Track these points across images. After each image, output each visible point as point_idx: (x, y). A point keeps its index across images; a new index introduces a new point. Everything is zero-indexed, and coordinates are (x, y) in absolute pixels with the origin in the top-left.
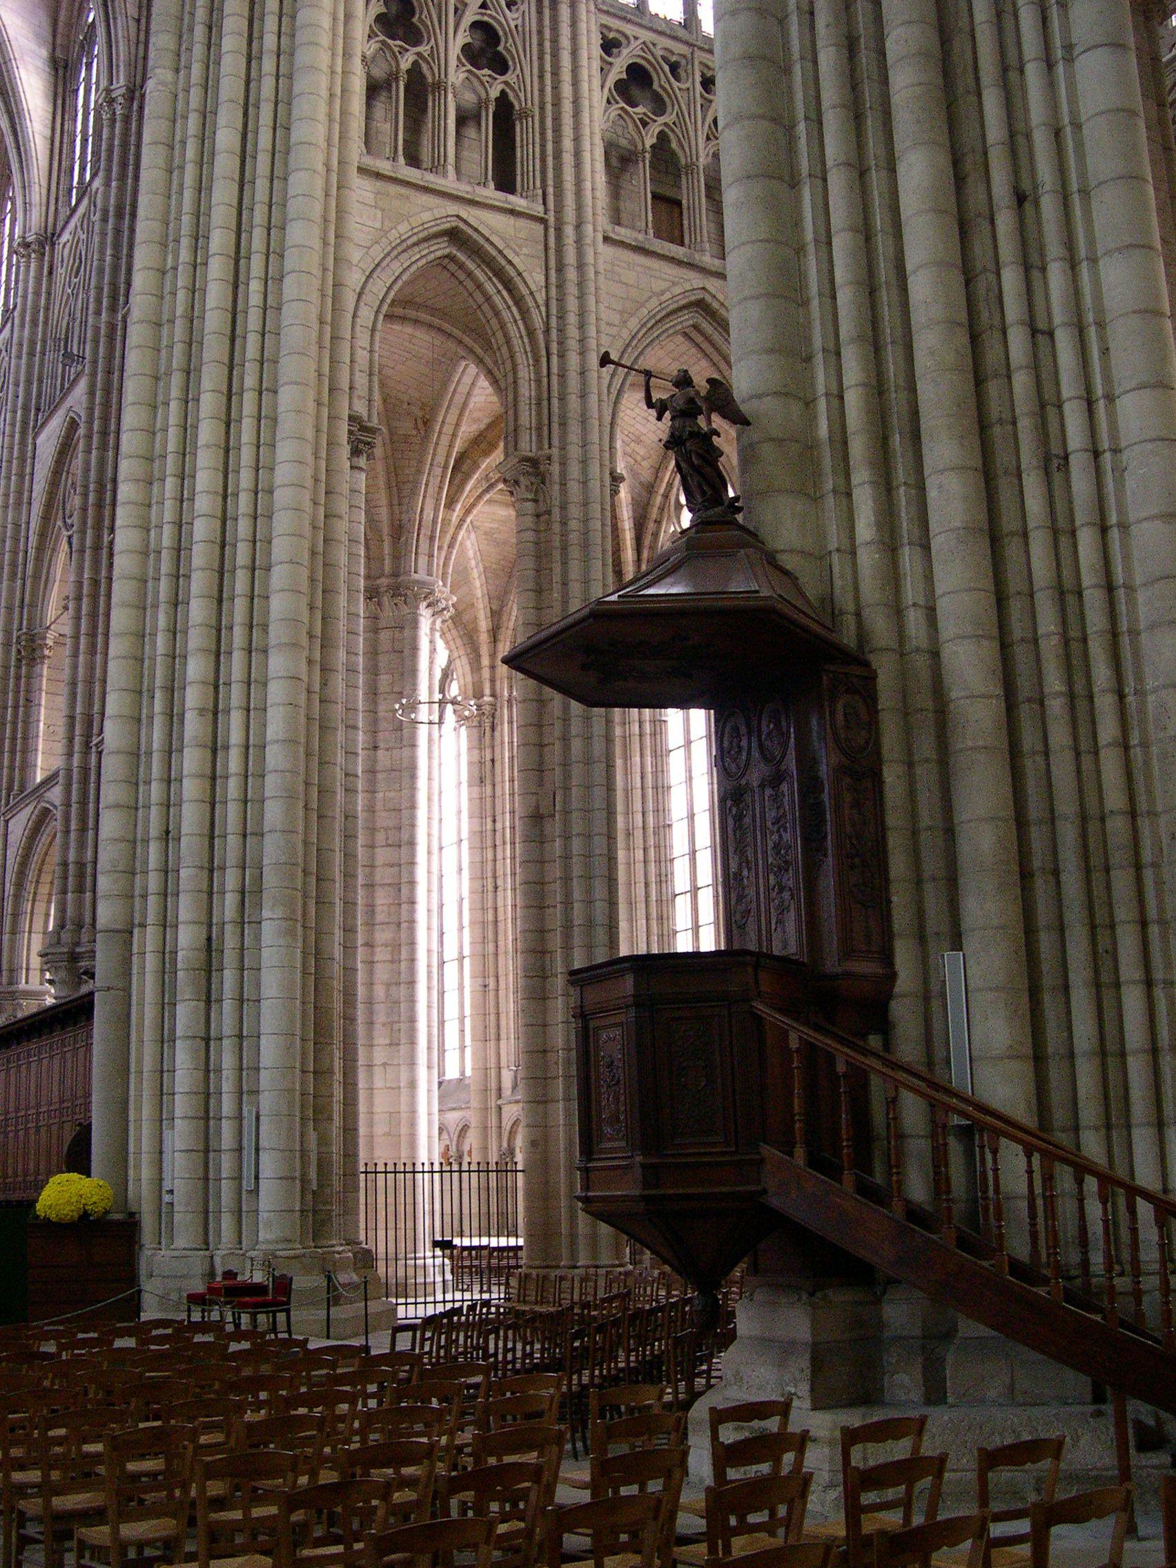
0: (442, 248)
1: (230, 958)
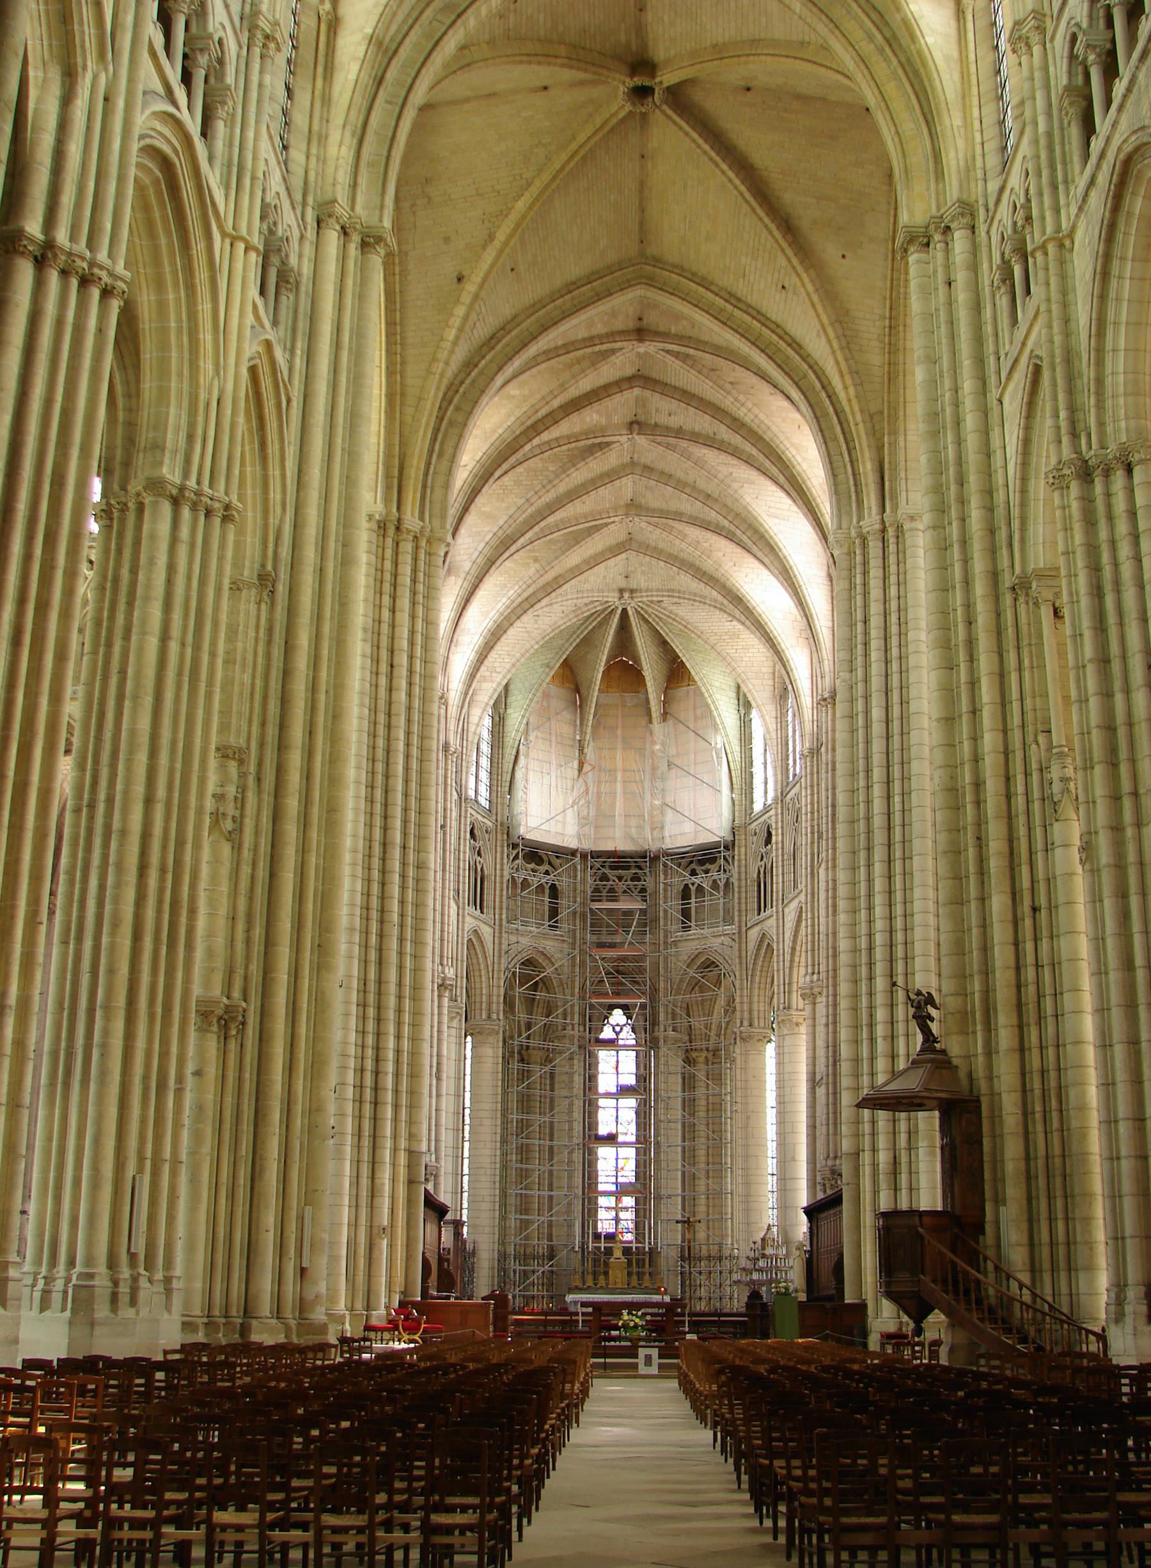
1: (904, 1168)
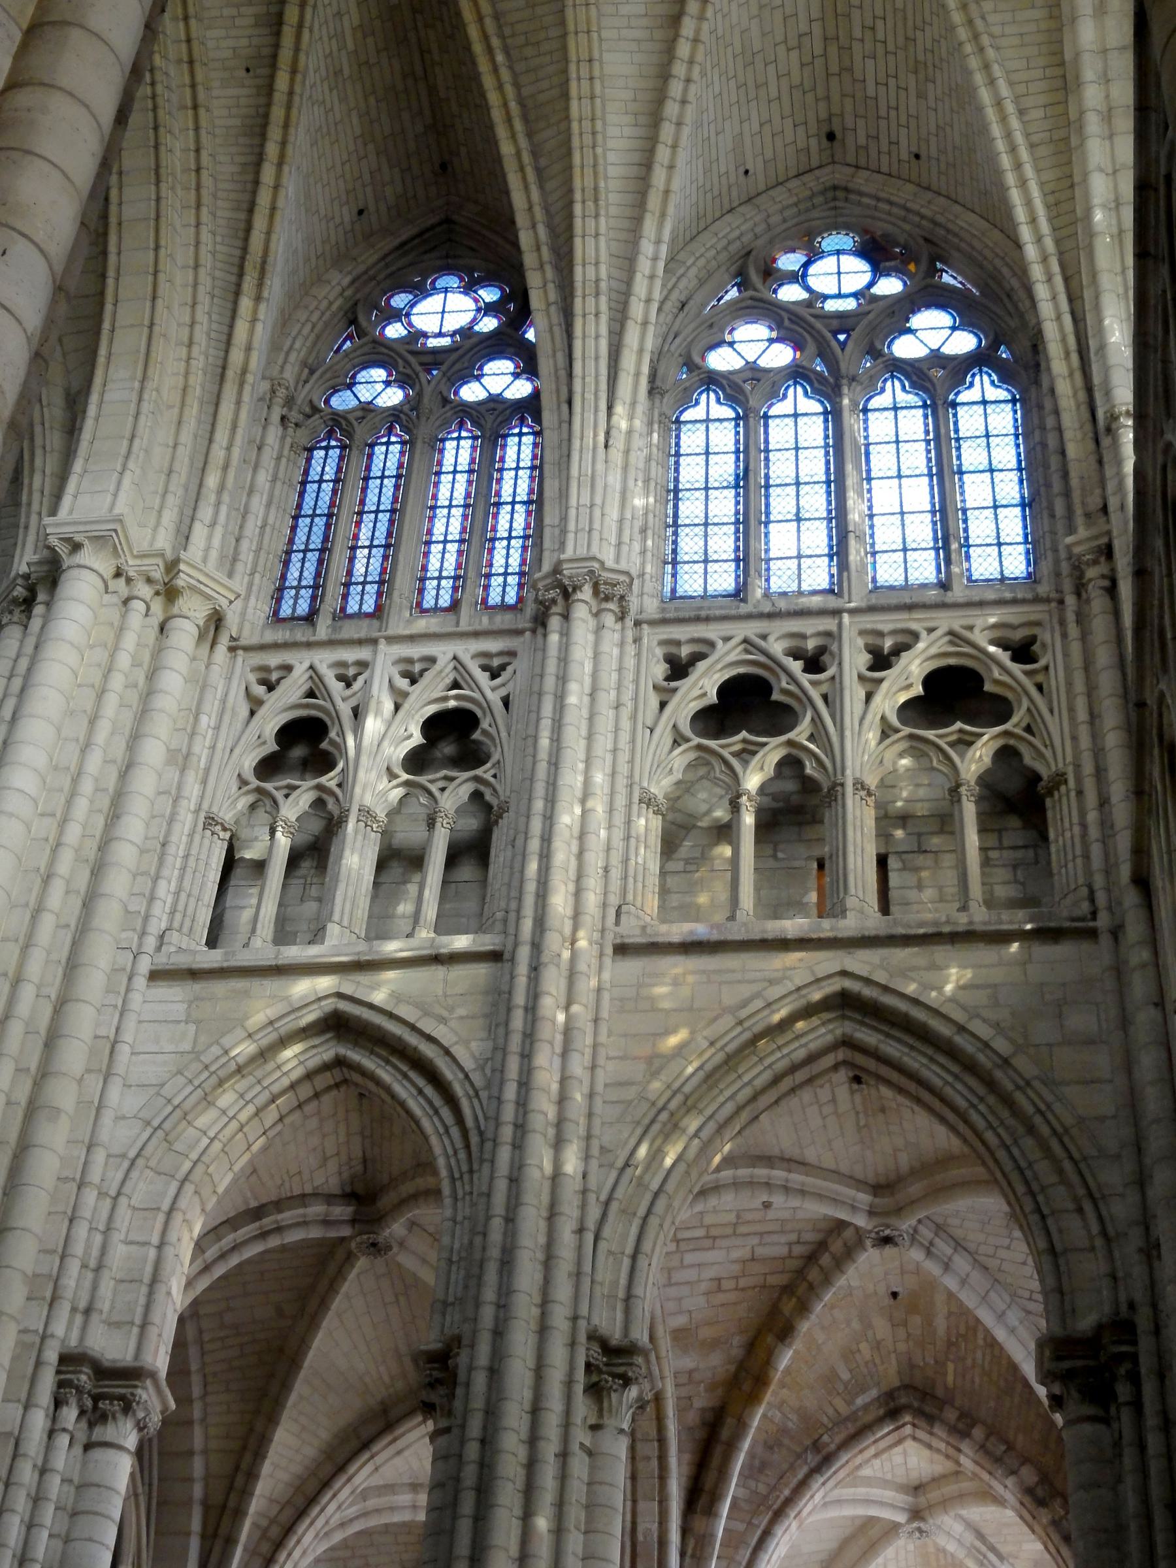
0: (327, 1051)
